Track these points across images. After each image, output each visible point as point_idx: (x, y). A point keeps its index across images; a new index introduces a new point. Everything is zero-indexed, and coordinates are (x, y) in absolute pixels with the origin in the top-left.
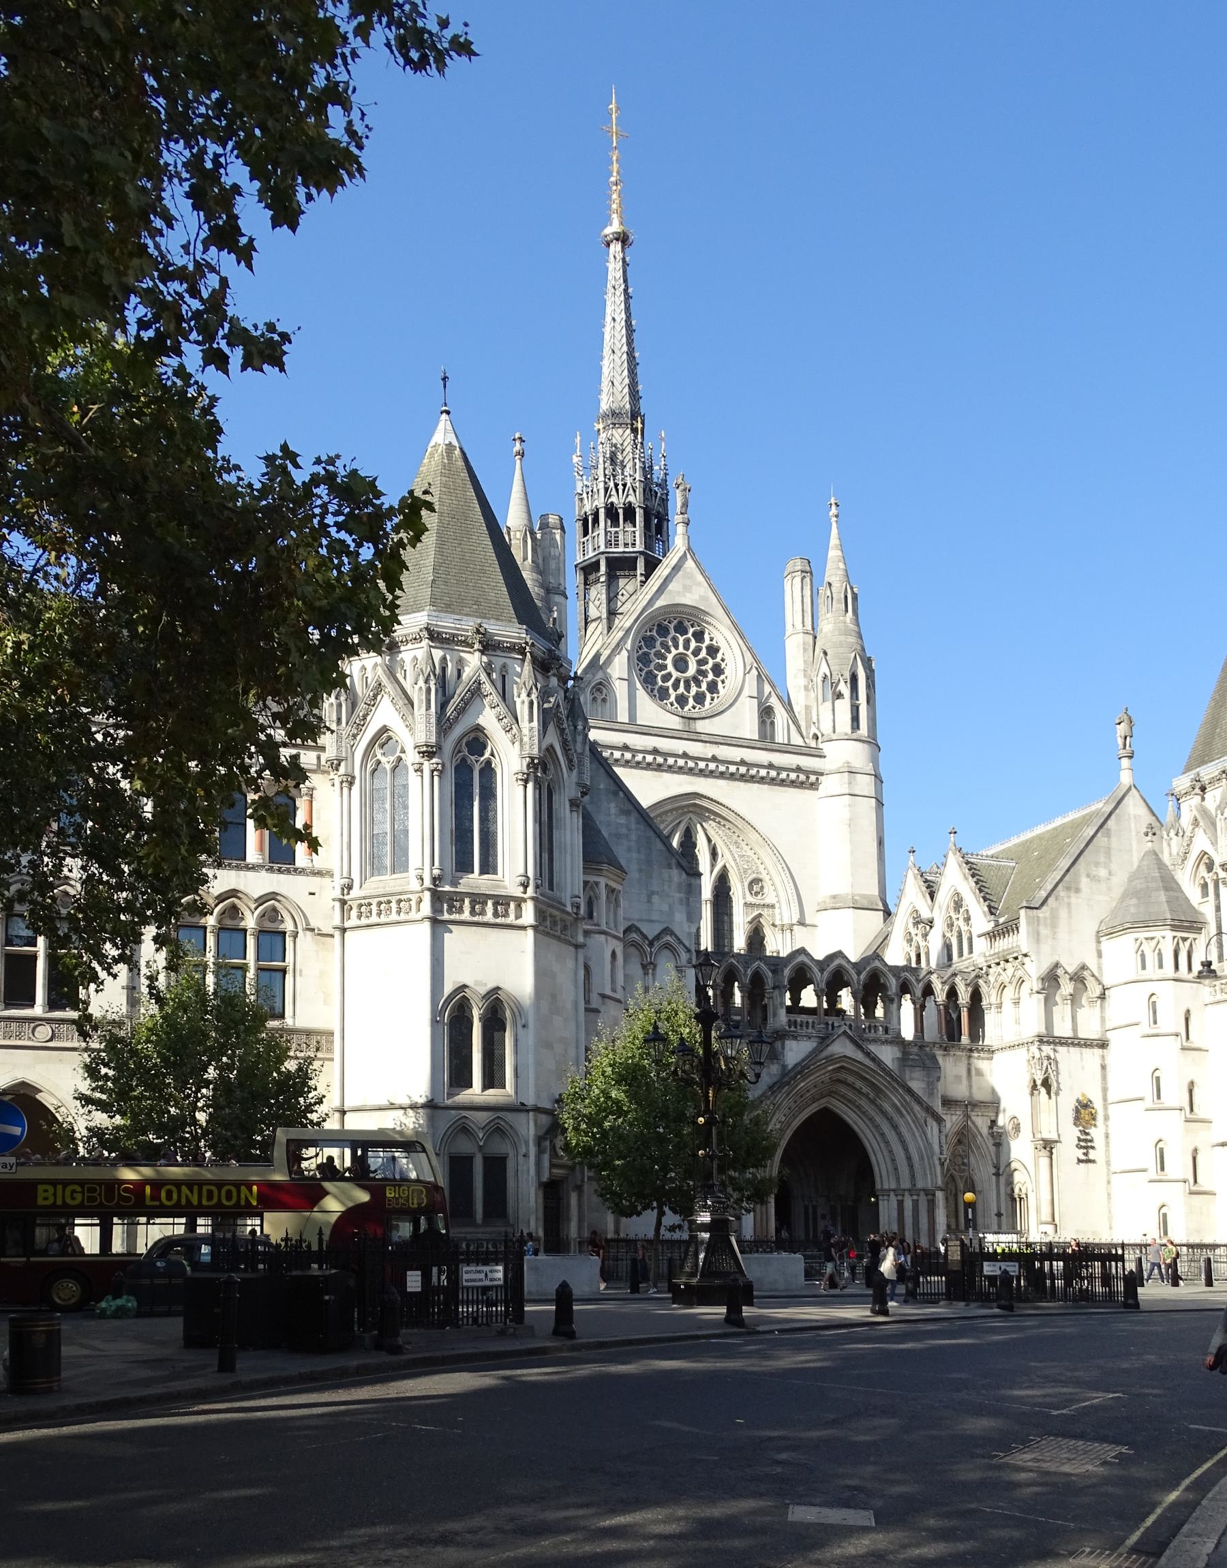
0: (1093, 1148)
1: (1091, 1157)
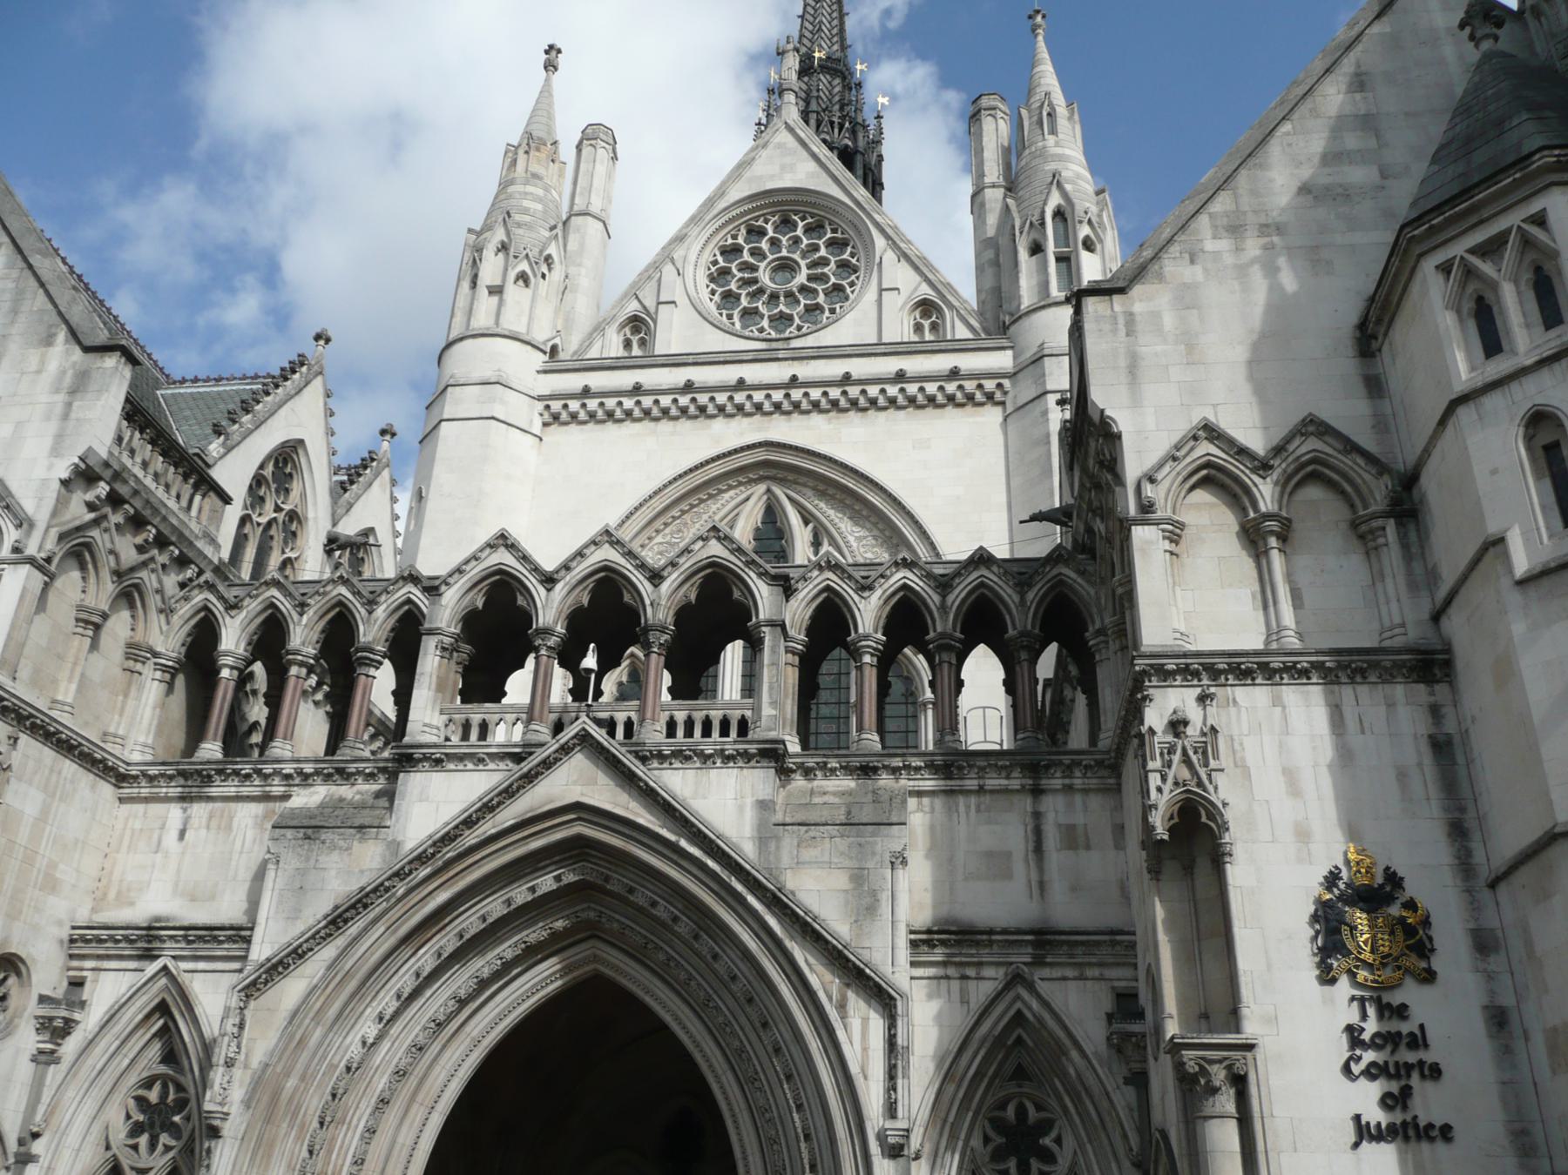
0: (1434, 1072)
1: (1429, 1104)
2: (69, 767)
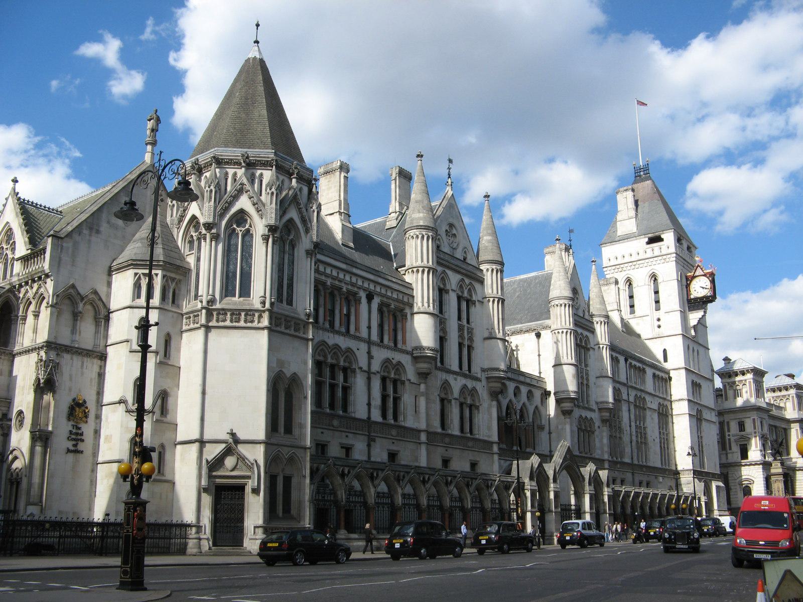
0: (83, 441)
1: (81, 446)
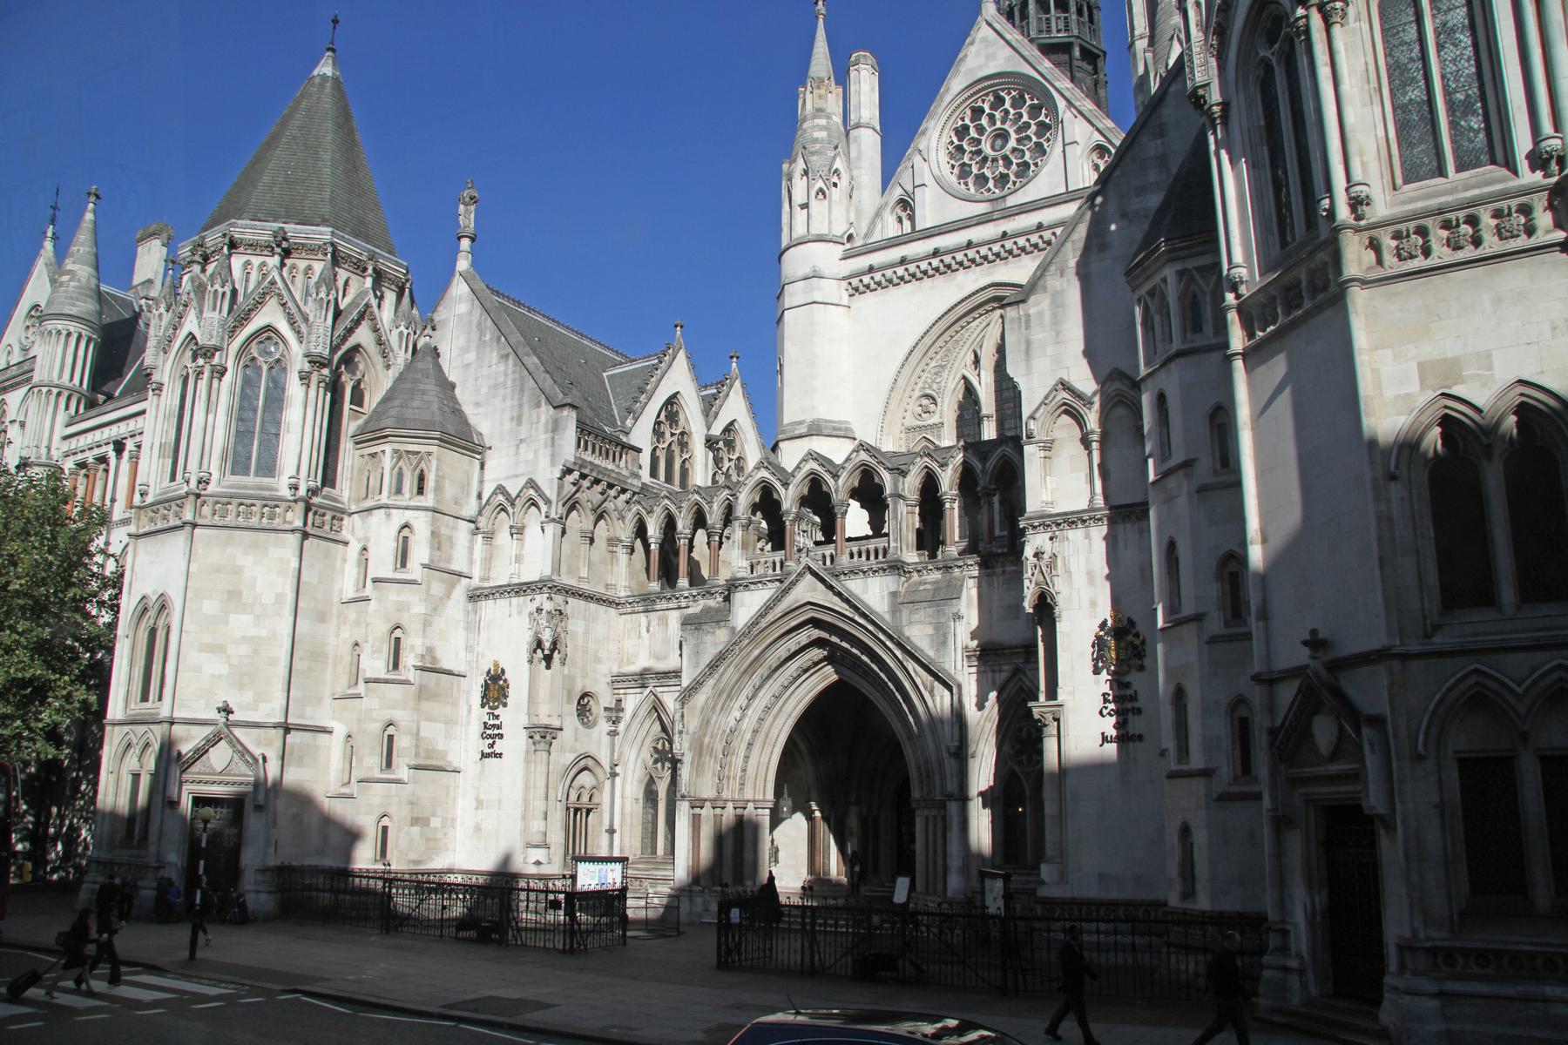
0: (1138, 711)
2: (593, 606)
